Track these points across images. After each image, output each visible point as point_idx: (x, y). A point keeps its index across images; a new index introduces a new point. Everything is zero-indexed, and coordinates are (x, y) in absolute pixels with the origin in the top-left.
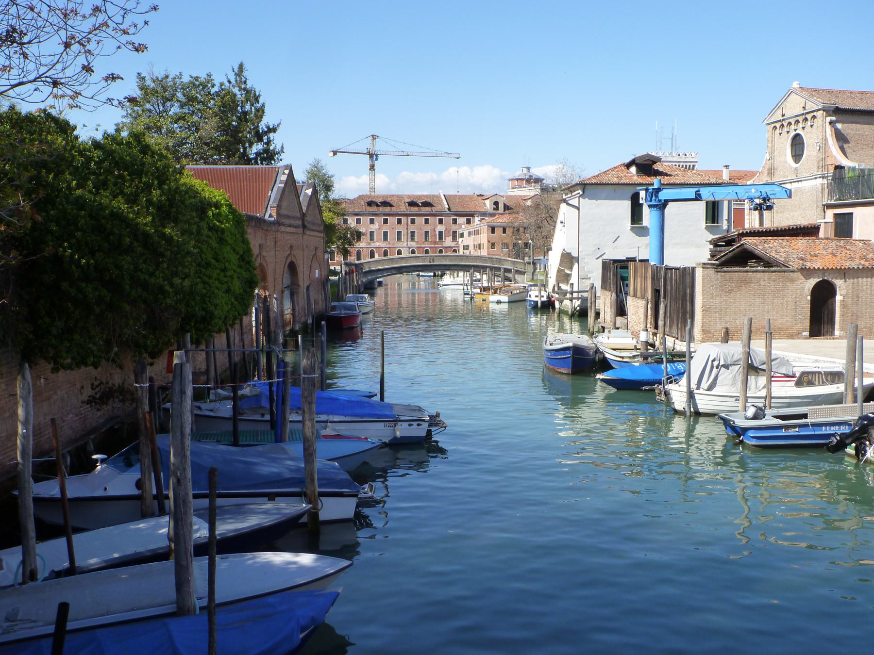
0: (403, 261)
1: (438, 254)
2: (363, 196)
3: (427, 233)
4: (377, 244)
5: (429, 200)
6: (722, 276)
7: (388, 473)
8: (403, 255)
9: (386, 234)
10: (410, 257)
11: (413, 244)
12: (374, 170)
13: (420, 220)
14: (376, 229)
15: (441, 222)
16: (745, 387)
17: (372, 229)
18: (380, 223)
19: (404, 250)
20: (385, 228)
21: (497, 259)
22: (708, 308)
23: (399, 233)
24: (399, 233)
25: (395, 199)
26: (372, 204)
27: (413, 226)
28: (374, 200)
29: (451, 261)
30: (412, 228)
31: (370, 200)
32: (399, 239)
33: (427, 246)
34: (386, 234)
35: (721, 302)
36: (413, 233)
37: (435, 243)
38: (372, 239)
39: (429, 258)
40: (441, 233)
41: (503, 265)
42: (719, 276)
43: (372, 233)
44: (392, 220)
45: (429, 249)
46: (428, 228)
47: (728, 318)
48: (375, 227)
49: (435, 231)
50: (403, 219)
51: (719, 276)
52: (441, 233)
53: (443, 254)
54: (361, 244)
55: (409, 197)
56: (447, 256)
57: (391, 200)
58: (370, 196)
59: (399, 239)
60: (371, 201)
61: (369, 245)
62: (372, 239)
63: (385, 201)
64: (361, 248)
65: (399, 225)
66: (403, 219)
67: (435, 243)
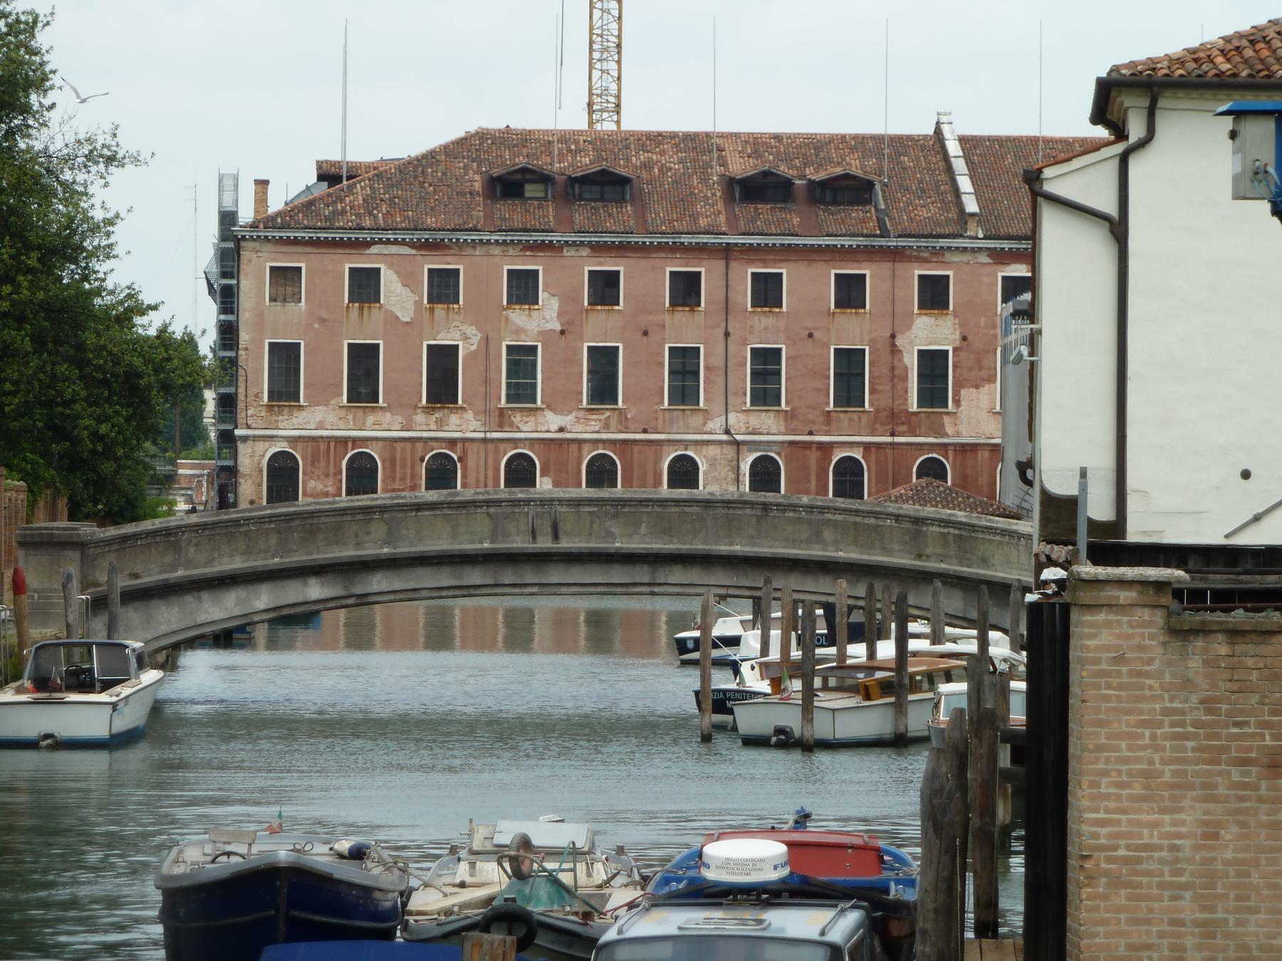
0: (378, 529)
1: (584, 491)
2: (482, 135)
3: (850, 362)
4: (551, 423)
5: (855, 166)
8: (462, 490)
9: (603, 361)
10: (419, 507)
14: (545, 335)
17: (519, 331)
18: (569, 300)
19: (713, 463)
21: (946, 523)
23: (685, 363)
24: (685, 363)
25: (672, 160)
26: (531, 190)
28: (542, 162)
29: (666, 530)
31: (521, 161)
34: (603, 361)
36: (766, 362)
38: (521, 392)
39: (532, 510)
40: (933, 363)
41: (984, 562)
45: (858, 454)
49: (894, 351)
50: (708, 271)
52: (933, 363)
53: (619, 491)
54: (454, 419)
55: (755, 144)
56: (642, 502)
57: (647, 166)
58: (601, 143)
60: (524, 170)
61: (501, 426)
62: (521, 392)
63: (603, 172)
64: (452, 443)
65: (682, 316)
66: (708, 271)
67: (895, 419)
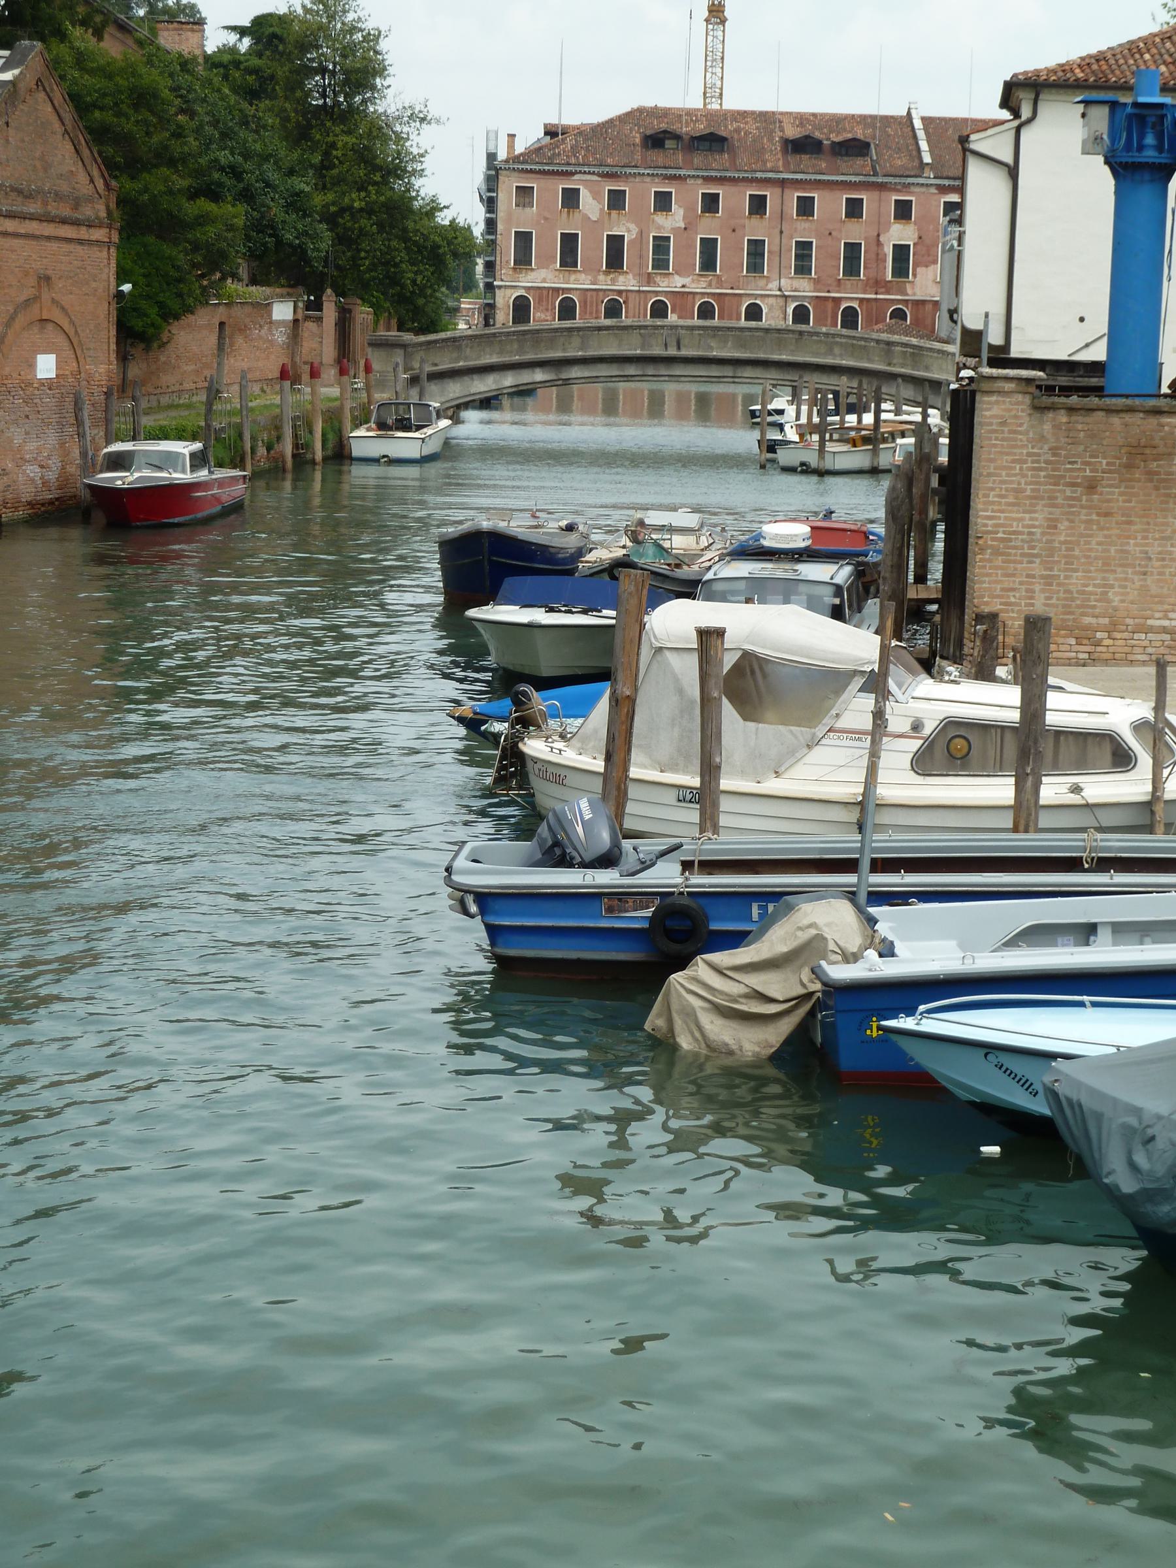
0: (576, 341)
1: (696, 321)
2: (640, 110)
3: (853, 250)
4: (677, 282)
5: (860, 133)
6: (1057, 427)
7: (491, 973)
8: (625, 320)
9: (709, 246)
10: (600, 329)
11: (804, 288)
12: (723, 21)
13: (831, 204)
14: (675, 230)
15: (903, 211)
16: (885, 808)
17: (659, 228)
18: (690, 209)
19: (771, 308)
20: (708, 227)
21: (906, 345)
22: (1002, 540)
23: (756, 248)
24: (756, 248)
25: (752, 127)
26: (669, 144)
27: (807, 225)
28: (675, 127)
29: (743, 346)
30: (757, 229)
31: (663, 126)
32: (756, 266)
33: (851, 296)
34: (709, 246)
35: (1052, 525)
36: (804, 249)
37: (878, 284)
38: (661, 263)
39: (665, 332)
40: (901, 252)
41: (927, 368)
42: (1047, 427)
43: (661, 244)
44: (734, 199)
45: (855, 305)
46: (855, 232)
47: (1076, 581)
48: (671, 222)
49: (879, 244)
50: (770, 194)
51: (1047, 427)
52: (901, 252)
53: (716, 322)
54: (621, 278)
55: (801, 119)
56: (729, 328)
57: (738, 130)
58: (710, 116)
59: (756, 266)
60: (665, 132)
61: (648, 284)
62: (661, 263)
63: (711, 134)
64: (620, 292)
65: (755, 220)
66: (770, 194)
67: (878, 284)
